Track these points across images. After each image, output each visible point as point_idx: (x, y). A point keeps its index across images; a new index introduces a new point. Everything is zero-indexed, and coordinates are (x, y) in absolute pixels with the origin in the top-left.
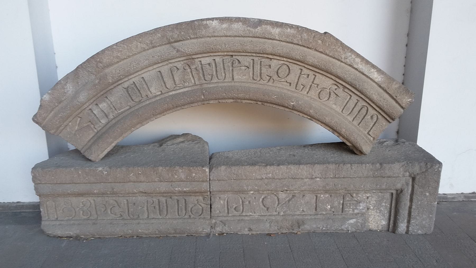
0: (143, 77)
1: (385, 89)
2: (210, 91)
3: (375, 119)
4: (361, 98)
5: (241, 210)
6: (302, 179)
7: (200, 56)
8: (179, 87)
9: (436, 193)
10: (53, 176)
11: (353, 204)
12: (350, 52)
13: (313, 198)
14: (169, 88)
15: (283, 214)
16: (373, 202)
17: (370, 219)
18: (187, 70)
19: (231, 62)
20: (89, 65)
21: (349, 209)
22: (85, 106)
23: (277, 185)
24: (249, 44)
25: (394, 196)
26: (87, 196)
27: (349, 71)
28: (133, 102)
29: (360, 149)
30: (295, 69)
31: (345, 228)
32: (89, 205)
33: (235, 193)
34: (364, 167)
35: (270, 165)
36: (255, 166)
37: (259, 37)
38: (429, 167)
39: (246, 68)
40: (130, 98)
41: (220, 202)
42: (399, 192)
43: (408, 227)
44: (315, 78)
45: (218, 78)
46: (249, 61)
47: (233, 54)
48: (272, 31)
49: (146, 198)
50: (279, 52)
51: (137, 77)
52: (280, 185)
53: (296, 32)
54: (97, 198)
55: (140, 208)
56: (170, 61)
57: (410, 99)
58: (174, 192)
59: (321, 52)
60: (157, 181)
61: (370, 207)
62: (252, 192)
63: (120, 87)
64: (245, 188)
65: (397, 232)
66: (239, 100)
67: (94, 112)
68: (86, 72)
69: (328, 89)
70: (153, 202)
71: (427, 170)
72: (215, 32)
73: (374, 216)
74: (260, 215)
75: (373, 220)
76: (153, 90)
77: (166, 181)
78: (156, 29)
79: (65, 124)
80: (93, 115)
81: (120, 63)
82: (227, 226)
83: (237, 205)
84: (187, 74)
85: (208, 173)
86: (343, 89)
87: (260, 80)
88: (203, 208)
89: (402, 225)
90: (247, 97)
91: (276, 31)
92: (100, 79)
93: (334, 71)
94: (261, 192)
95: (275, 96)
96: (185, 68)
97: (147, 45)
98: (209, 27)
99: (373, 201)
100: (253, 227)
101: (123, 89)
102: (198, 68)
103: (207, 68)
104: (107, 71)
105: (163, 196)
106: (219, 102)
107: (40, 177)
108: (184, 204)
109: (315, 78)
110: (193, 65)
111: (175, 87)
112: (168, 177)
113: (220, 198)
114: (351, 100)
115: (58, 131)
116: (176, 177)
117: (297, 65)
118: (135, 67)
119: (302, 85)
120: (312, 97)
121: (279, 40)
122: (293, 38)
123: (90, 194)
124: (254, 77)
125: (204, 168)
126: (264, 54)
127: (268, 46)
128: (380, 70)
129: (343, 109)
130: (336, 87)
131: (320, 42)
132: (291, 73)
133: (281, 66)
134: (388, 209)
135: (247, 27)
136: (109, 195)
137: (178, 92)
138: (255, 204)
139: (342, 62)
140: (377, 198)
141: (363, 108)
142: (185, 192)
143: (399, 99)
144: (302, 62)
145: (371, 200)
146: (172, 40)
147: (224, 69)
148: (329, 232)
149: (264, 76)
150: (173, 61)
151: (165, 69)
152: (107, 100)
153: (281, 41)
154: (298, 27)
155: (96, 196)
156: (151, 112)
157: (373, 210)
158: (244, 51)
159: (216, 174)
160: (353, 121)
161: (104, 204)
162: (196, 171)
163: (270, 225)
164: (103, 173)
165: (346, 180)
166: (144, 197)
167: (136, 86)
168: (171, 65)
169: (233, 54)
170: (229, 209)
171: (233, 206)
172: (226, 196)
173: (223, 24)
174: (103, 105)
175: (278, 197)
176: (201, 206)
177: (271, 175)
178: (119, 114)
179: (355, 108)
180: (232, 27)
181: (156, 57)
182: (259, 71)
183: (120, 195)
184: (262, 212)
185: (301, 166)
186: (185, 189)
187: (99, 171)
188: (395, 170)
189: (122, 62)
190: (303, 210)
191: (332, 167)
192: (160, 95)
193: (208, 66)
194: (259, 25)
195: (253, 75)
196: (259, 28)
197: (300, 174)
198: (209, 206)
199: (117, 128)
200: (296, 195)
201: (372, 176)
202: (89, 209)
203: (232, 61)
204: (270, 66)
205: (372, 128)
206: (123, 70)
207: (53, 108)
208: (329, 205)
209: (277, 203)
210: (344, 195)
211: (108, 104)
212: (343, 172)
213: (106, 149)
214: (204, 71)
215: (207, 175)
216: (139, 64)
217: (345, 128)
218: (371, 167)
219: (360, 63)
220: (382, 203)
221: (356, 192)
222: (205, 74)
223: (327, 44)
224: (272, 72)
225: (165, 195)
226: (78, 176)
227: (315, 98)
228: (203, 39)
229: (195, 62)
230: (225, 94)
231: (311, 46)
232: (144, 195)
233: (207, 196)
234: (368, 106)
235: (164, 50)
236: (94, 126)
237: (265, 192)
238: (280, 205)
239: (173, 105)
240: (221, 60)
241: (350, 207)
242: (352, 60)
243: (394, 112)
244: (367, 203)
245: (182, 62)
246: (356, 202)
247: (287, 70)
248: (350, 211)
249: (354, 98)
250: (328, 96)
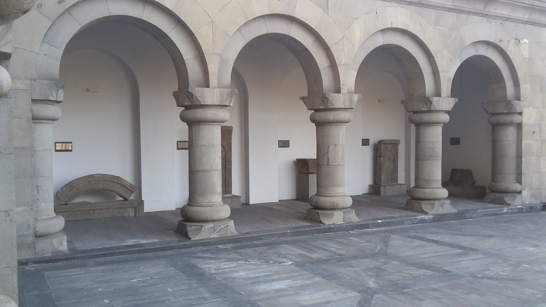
30: (112, 183)
91: (108, 176)
144: (114, 182)
174: (71, 192)
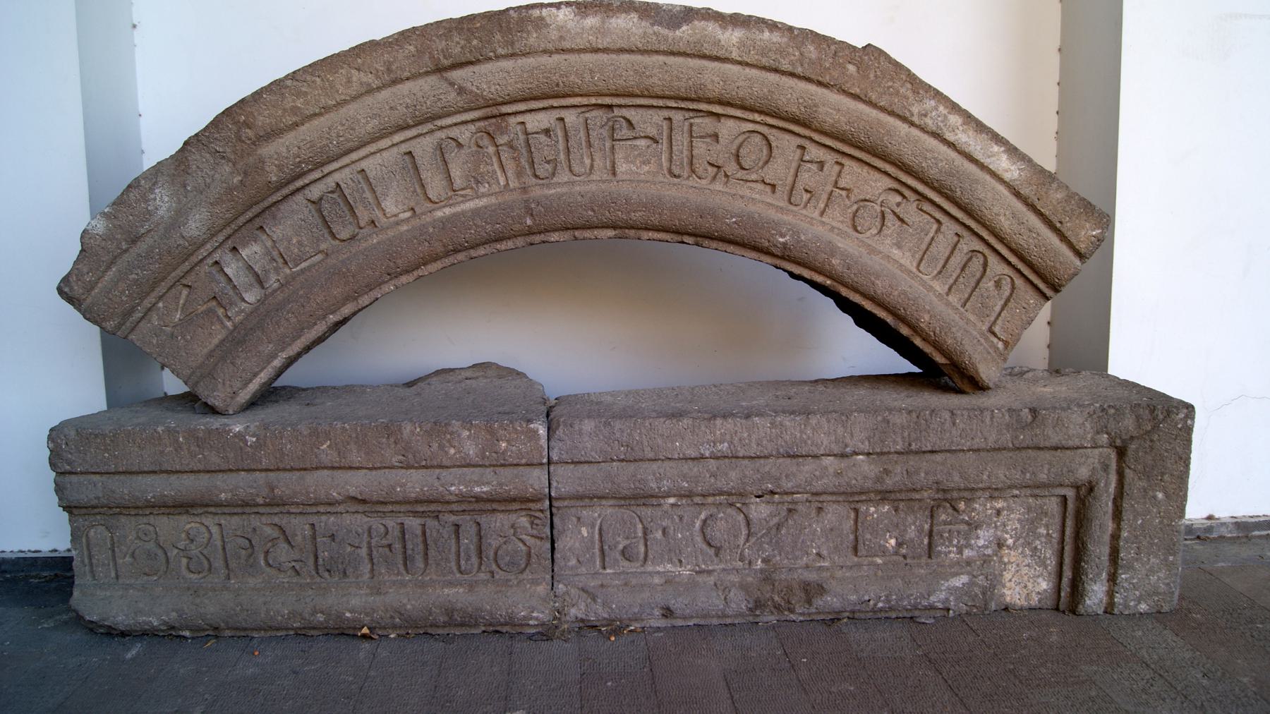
0: (363, 170)
1: (1030, 201)
2: (549, 203)
3: (1006, 290)
4: (968, 228)
5: (642, 556)
6: (815, 457)
7: (522, 107)
8: (462, 196)
9: (1181, 491)
10: (106, 450)
11: (959, 532)
12: (934, 98)
13: (848, 517)
14: (434, 199)
15: (763, 566)
16: (1014, 525)
17: (1007, 576)
18: (487, 148)
19: (607, 128)
20: (216, 135)
22: (203, 252)
23: (745, 476)
24: (659, 72)
25: (1071, 506)
26: (200, 511)
27: (931, 151)
28: (333, 242)
29: (972, 372)
30: (786, 144)
31: (939, 602)
32: (205, 540)
33: (623, 502)
34: (988, 420)
35: (724, 417)
36: (681, 418)
37: (685, 54)
38: (1161, 417)
39: (649, 142)
40: (325, 231)
41: (580, 532)
42: (1083, 491)
43: (1111, 594)
44: (840, 172)
45: (571, 170)
46: (657, 124)
47: (616, 101)
48: (721, 37)
49: (367, 519)
50: (741, 94)
51: (347, 170)
52: (754, 477)
53: (785, 40)
54: (228, 518)
55: (349, 549)
56: (439, 123)
57: (1099, 229)
58: (447, 498)
59: (855, 97)
60: (397, 464)
61: (1006, 540)
62: (672, 500)
63: (299, 198)
64: (651, 485)
65: (1081, 609)
66: (632, 233)
67: (225, 269)
68: (208, 155)
69: (879, 202)
70: (387, 533)
71: (1155, 427)
72: (564, 40)
73: (1018, 565)
75: (1013, 580)
76: (390, 206)
77: (424, 463)
78: (402, 33)
79: (147, 303)
80: (222, 279)
81: (302, 128)
82: (599, 600)
83: (628, 542)
84: (485, 158)
85: (543, 442)
86: (918, 205)
87: (689, 177)
88: (529, 547)
89: (1095, 588)
90: (655, 220)
92: (245, 173)
93: (892, 149)
94: (697, 500)
95: (732, 217)
96: (481, 143)
97: (377, 77)
98: (547, 26)
99: (1014, 520)
100: (677, 604)
101: (309, 204)
102: (515, 143)
103: (540, 143)
104: (268, 150)
105: (416, 514)
106: (576, 238)
107: (71, 453)
108: (475, 540)
109: (840, 172)
110: (502, 134)
111: (450, 198)
112: (429, 453)
113: (579, 519)
114: (941, 236)
115: (128, 324)
116: (452, 451)
117: (791, 135)
118: (341, 139)
119: (807, 191)
120: (834, 224)
121: (740, 63)
122: (778, 56)
123: (207, 505)
124: (673, 167)
125: (532, 426)
126: (698, 100)
127: (712, 76)
128: (1016, 149)
129: (921, 260)
130: (898, 199)
131: (852, 68)
132: (774, 158)
133: (749, 137)
134: (1056, 546)
135: (652, 25)
136: (261, 510)
137: (458, 209)
138: (679, 535)
139: (912, 124)
140: (1023, 514)
141: (974, 259)
142: (478, 499)
143: (1068, 230)
145: (1009, 520)
146: (446, 62)
147: (590, 145)
148: (894, 616)
149: (700, 166)
150: (449, 121)
152: (264, 237)
153: (747, 64)
154: (791, 29)
155: (226, 510)
156: (382, 265)
157: (1014, 548)
158: (646, 93)
159: (568, 442)
160: (947, 295)
161: (249, 536)
162: (510, 434)
163: (725, 599)
164: (247, 441)
165: (938, 457)
166: (359, 516)
167: (345, 195)
168: (441, 135)
169: (616, 101)
170: (606, 553)
171: (618, 543)
172: (596, 515)
174: (252, 251)
175: (746, 517)
176: (525, 544)
177: (726, 444)
178: (294, 277)
179: (952, 259)
180: (610, 24)
181: (402, 109)
182: (686, 153)
183: (291, 510)
184: (700, 558)
186: (477, 489)
187: (235, 436)
188: (1072, 426)
189: (307, 125)
190: (819, 554)
191: (898, 421)
192: (408, 220)
193: (543, 138)
194: (685, 22)
195: (671, 161)
196: (684, 28)
197: (809, 442)
198: (548, 545)
199: (288, 313)
200: (797, 507)
201: (1011, 446)
202: (205, 552)
203: (611, 123)
204: (716, 137)
205: (999, 314)
206: (308, 146)
207: (115, 257)
208: (891, 537)
209: (743, 533)
210: (933, 507)
211: (266, 247)
212: (932, 435)
213: (255, 375)
214: (533, 150)
215: (541, 446)
216: (354, 129)
217: (929, 312)
219: (961, 128)
220: (1037, 528)
221: (966, 494)
222: (535, 160)
223: (872, 76)
224: (720, 152)
225: (420, 508)
226: (176, 450)
227: (846, 229)
228: (530, 61)
229: (507, 127)
230: (594, 211)
231: (828, 78)
232: (361, 508)
233: (542, 511)
234: (987, 252)
235: (426, 89)
236: (226, 310)
237: (710, 500)
238: (753, 540)
239: (444, 246)
240: (581, 120)
241: (951, 541)
242: (939, 119)
243: (1058, 265)
244: (996, 527)
245: (472, 127)
246: (966, 528)
247: (765, 151)
248: (950, 552)
249: (950, 228)
250: (878, 224)
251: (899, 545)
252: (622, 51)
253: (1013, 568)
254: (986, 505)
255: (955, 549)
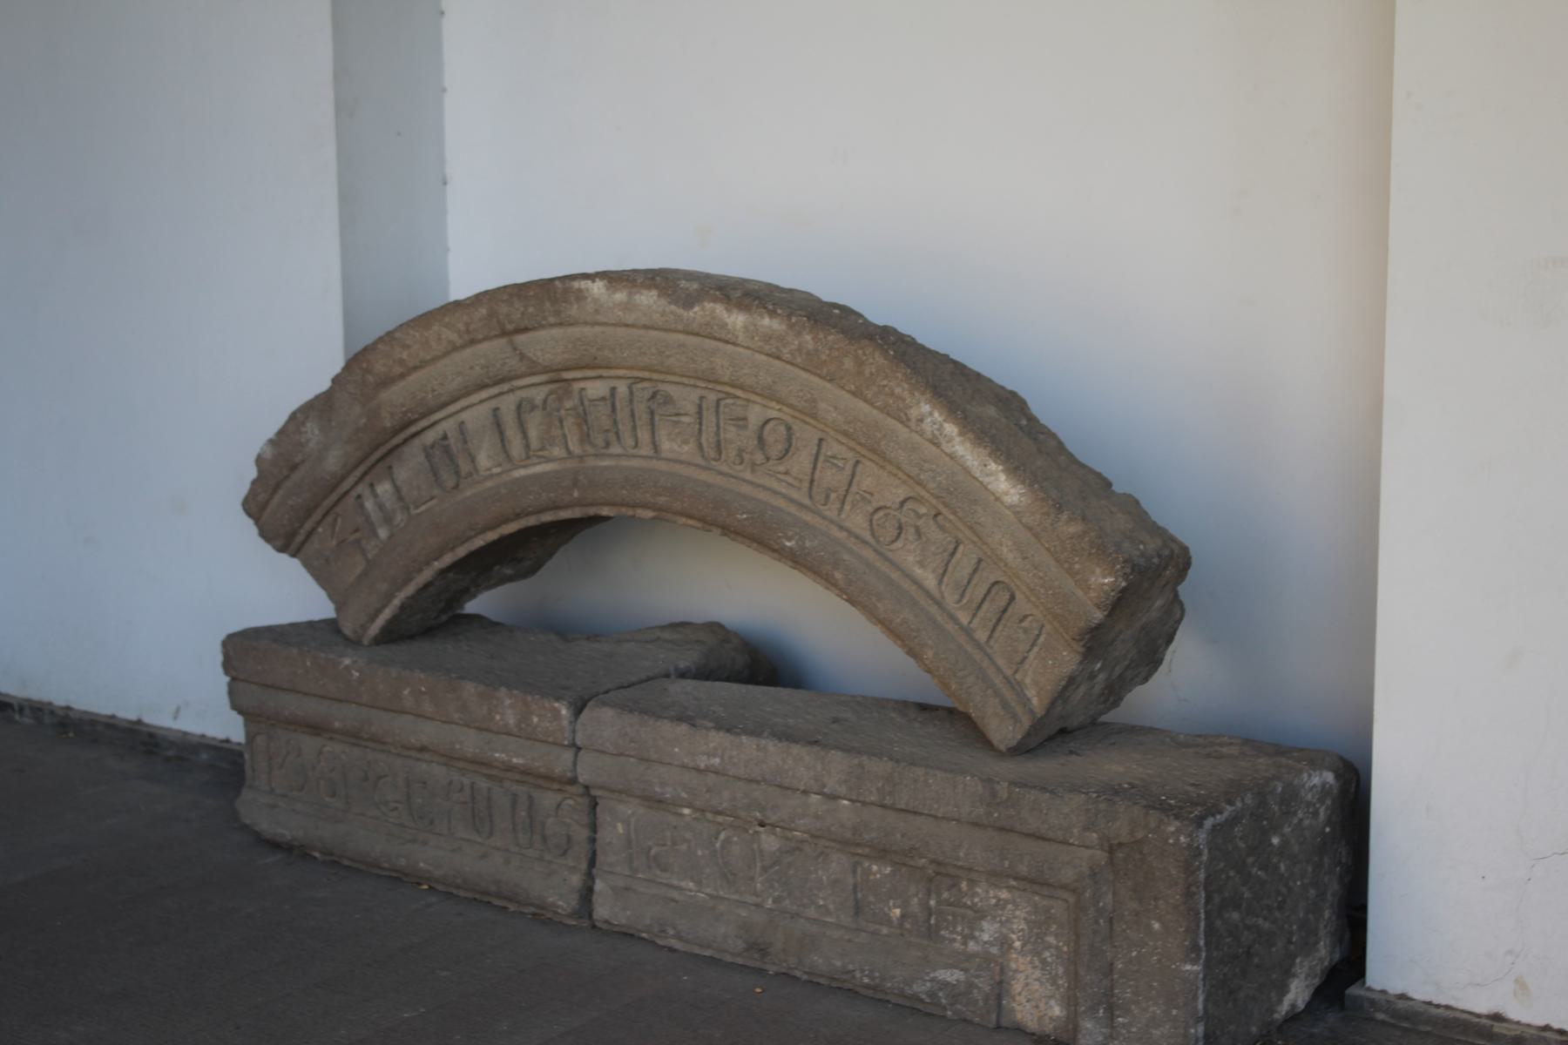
17: (1017, 986)
21: (951, 933)
48: (728, 321)
53: (784, 327)
73: (1027, 977)
74: (715, 893)
91: (737, 320)
95: (744, 513)
98: (585, 298)
99: (1020, 922)
104: (385, 396)
135: (670, 303)
145: (1015, 917)
151: (508, 404)
157: (1021, 952)
173: (616, 290)
177: (717, 760)
185: (796, 749)
186: (515, 760)
196: (696, 309)
208: (895, 907)
218: (980, 788)
219: (958, 439)
223: (867, 373)
228: (575, 331)
241: (955, 927)
251: (903, 916)
252: (646, 327)
253: (1021, 977)
254: (987, 892)
255: (959, 938)
